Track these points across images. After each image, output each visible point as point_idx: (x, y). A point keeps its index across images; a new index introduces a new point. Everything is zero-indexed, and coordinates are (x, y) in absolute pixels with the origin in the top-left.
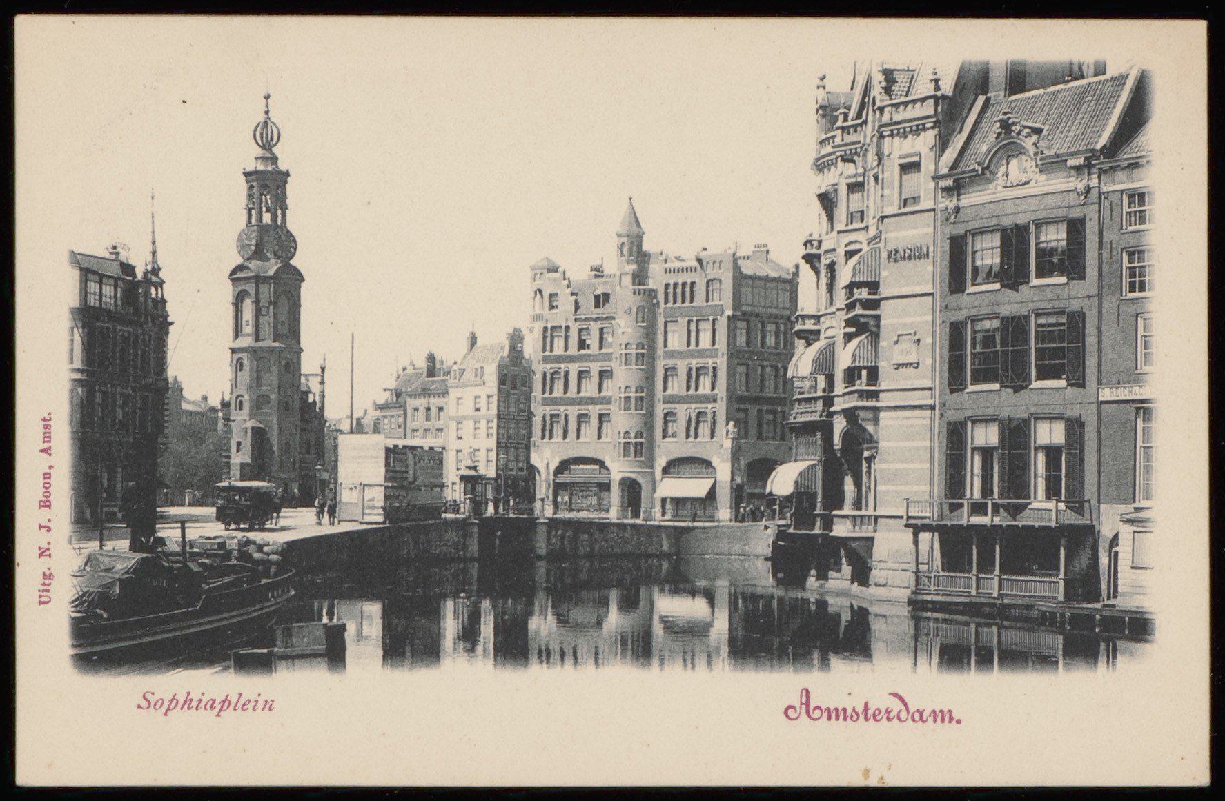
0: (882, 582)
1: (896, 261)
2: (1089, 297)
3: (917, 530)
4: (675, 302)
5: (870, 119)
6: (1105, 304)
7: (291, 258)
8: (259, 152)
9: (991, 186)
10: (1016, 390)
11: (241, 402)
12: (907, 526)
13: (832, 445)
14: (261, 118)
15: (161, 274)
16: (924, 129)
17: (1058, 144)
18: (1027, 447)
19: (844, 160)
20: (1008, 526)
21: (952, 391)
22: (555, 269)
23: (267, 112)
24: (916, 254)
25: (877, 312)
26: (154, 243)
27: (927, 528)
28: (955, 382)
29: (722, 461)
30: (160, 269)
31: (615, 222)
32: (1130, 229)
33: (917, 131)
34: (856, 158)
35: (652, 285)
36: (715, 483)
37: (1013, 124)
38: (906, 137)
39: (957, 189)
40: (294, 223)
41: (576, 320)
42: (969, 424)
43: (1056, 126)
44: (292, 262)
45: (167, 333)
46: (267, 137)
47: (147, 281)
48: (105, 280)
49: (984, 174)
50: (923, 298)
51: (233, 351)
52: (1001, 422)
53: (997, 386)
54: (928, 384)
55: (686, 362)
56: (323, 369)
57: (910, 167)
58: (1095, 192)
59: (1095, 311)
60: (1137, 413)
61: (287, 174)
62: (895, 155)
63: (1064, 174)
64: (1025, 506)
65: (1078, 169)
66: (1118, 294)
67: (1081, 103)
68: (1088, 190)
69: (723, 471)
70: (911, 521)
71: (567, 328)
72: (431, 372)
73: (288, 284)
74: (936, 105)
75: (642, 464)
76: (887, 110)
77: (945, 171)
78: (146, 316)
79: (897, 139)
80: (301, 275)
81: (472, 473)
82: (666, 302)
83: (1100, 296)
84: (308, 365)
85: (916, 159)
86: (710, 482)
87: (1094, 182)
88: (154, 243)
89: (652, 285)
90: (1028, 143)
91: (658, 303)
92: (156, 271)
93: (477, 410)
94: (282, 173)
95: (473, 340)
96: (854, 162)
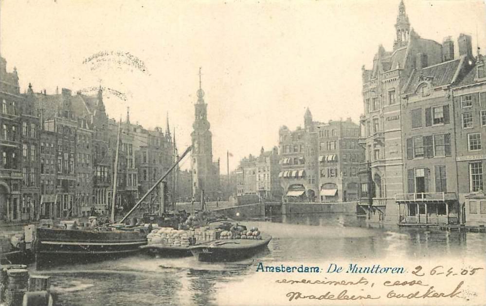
5: (379, 78)
7: (209, 128)
13: (371, 178)
23: (200, 87)
29: (340, 184)
36: (337, 191)
40: (208, 120)
44: (209, 130)
46: (201, 94)
56: (219, 161)
69: (340, 187)
70: (398, 201)
73: (208, 137)
81: (262, 190)
83: (455, 129)
85: (394, 89)
86: (335, 190)
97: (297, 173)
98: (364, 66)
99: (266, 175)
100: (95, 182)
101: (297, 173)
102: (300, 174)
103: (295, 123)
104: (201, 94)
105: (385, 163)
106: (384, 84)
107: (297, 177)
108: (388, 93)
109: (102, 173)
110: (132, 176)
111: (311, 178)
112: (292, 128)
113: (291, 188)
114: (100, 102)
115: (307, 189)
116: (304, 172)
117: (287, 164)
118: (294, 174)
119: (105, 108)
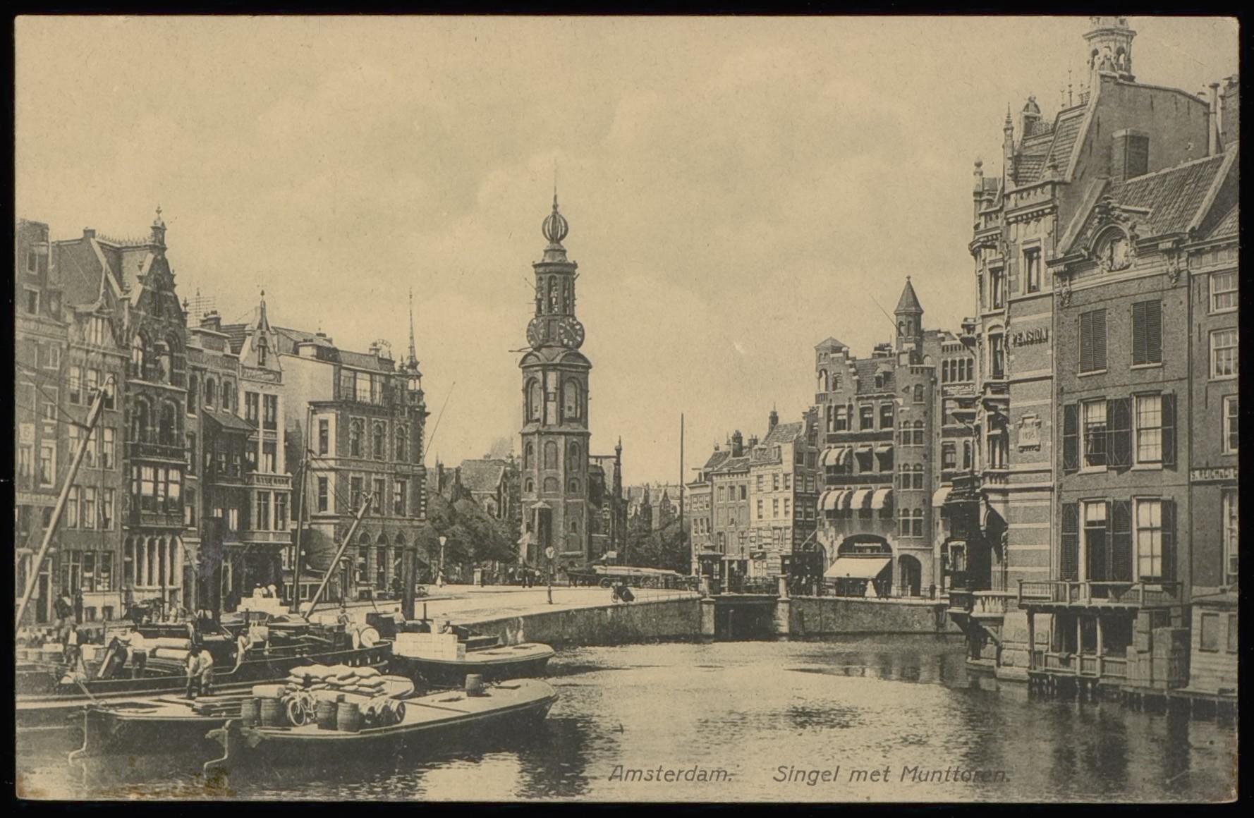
0: (1009, 661)
1: (1021, 345)
2: (1180, 379)
3: (1032, 611)
4: (953, 379)
6: (1195, 386)
7: (580, 344)
8: (546, 244)
9: (1096, 270)
10: (1120, 471)
11: (531, 485)
12: (1021, 607)
14: (550, 211)
15: (419, 368)
16: (1044, 215)
17: (1145, 232)
18: (1129, 527)
19: (986, 247)
20: (1116, 608)
21: (1068, 473)
22: (837, 349)
24: (1037, 339)
25: (1006, 396)
26: (412, 338)
27: (1047, 609)
28: (1069, 462)
30: (417, 363)
31: (893, 298)
32: (1217, 311)
33: (1038, 216)
34: (997, 244)
35: (928, 363)
37: (1113, 208)
38: (1028, 223)
39: (1067, 275)
40: (582, 311)
41: (858, 399)
42: (1082, 505)
43: (1159, 209)
44: (581, 350)
45: (423, 423)
46: (556, 231)
47: (403, 374)
48: (359, 375)
49: (1088, 262)
50: (1044, 382)
51: (524, 435)
52: (1108, 504)
53: (1103, 468)
54: (1047, 466)
55: (964, 439)
57: (1031, 254)
58: (1184, 274)
59: (1186, 393)
60: (1223, 497)
61: (575, 266)
62: (1020, 241)
63: (1157, 258)
64: (1129, 587)
65: (1166, 251)
66: (1205, 377)
67: (1182, 185)
68: (1179, 272)
70: (1026, 602)
71: (851, 407)
72: (738, 452)
73: (575, 371)
74: (1053, 189)
75: (920, 541)
76: (1013, 196)
77: (1061, 256)
78: (403, 407)
79: (1021, 226)
80: (586, 361)
82: (944, 379)
83: (1190, 379)
84: (599, 446)
86: (886, 561)
87: (1183, 265)
88: (412, 338)
89: (928, 363)
90: (1125, 228)
91: (936, 380)
92: (413, 365)
93: (776, 488)
94: (569, 265)
95: (774, 418)
96: (995, 247)
97: (869, 498)
98: (979, 165)
99: (781, 504)
100: (134, 517)
101: (869, 498)
102: (878, 501)
103: (870, 331)
104: (556, 231)
105: (1007, 482)
106: (1013, 226)
107: (866, 512)
108: (1022, 254)
109: (161, 486)
110: (272, 497)
111: (911, 518)
112: (862, 350)
113: (847, 549)
114: (155, 260)
115: (896, 554)
116: (889, 497)
117: (837, 468)
118: (857, 502)
119: (176, 281)
